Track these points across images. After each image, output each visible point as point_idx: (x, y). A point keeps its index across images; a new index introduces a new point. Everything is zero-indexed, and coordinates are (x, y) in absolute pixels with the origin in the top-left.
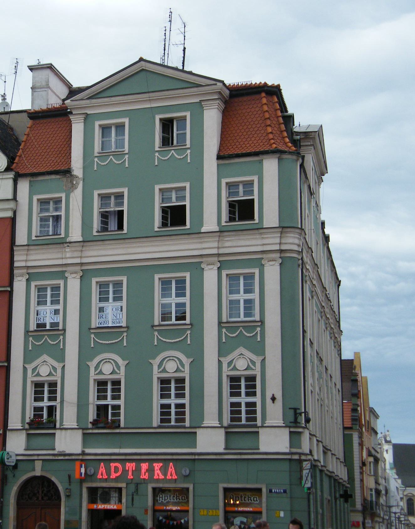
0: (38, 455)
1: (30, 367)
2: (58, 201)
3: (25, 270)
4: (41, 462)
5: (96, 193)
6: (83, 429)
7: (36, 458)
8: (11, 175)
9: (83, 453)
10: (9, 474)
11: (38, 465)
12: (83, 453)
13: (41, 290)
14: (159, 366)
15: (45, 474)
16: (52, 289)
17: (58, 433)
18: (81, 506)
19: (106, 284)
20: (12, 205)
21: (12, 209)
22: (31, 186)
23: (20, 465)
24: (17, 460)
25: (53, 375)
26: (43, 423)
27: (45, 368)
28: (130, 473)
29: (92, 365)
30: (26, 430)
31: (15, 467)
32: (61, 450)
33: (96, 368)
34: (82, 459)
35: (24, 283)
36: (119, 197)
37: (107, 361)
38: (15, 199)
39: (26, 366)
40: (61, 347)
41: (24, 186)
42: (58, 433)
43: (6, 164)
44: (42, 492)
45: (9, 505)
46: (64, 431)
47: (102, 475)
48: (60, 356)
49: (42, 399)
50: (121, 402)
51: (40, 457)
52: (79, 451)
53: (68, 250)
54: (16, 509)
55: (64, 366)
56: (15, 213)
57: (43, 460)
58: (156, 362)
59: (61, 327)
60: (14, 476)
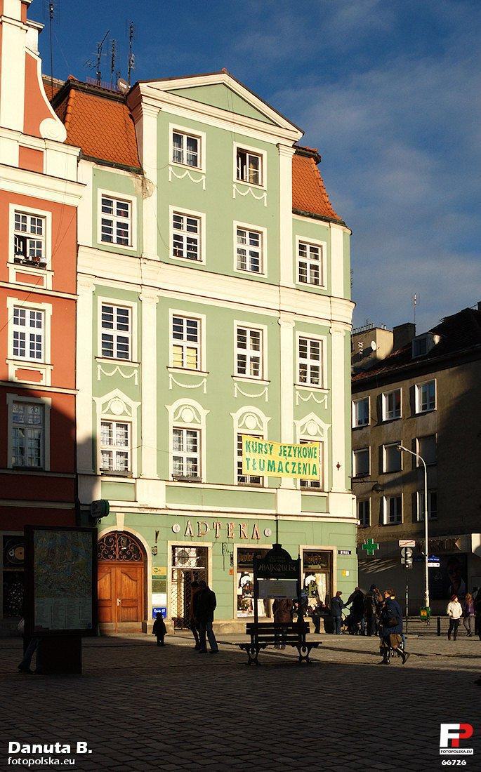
14: (240, 421)
25: (127, 415)
29: (171, 409)
33: (176, 413)
40: (136, 383)
43: (40, 128)
44: (120, 549)
48: (136, 393)
58: (236, 416)
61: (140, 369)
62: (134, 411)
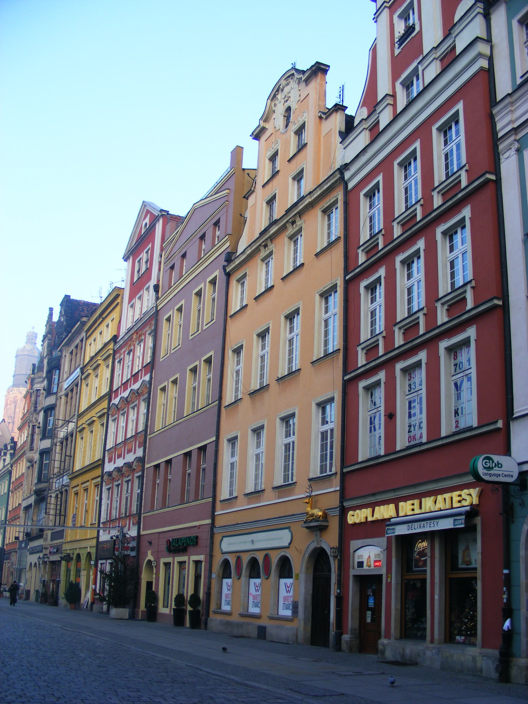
3: (512, 138)
56: (491, 59)
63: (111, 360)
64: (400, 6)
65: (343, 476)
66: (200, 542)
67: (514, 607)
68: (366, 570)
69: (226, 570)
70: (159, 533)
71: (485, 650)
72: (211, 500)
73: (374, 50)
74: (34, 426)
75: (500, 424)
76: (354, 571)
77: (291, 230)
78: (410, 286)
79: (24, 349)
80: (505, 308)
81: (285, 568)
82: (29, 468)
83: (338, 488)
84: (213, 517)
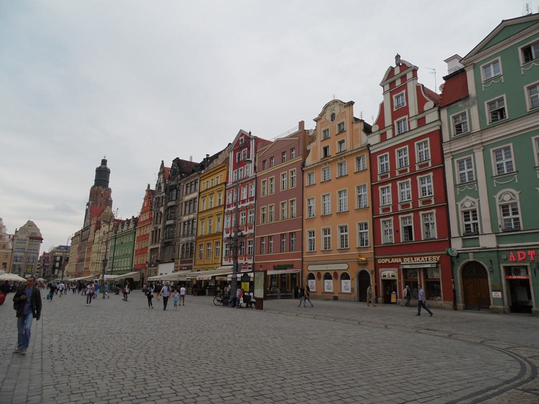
0: (470, 250)
1: (459, 204)
2: (464, 114)
4: (472, 253)
5: (486, 103)
6: (496, 233)
7: (469, 251)
8: (436, 109)
9: (498, 247)
10: (455, 260)
11: (471, 255)
12: (498, 247)
13: (461, 162)
15: (475, 260)
16: (467, 161)
17: (480, 237)
18: (501, 277)
19: (500, 150)
20: (438, 123)
21: (438, 125)
22: (448, 112)
23: (460, 255)
24: (458, 253)
25: (473, 206)
26: (471, 233)
27: (468, 203)
28: (532, 257)
29: (497, 197)
30: (462, 237)
31: (458, 257)
32: (484, 246)
33: (500, 198)
34: (498, 251)
35: (450, 161)
36: (501, 100)
37: (507, 193)
38: (440, 119)
39: (457, 203)
41: (444, 113)
42: (480, 237)
45: (457, 278)
46: (484, 236)
47: (512, 259)
48: (476, 195)
49: (469, 220)
50: (519, 216)
51: (471, 251)
52: (495, 246)
53: (473, 137)
54: (462, 280)
55: (479, 200)
56: (441, 127)
57: (473, 252)
59: (474, 180)
60: (458, 262)
61: (477, 183)
62: (477, 203)
63: (222, 193)
64: (397, 93)
65: (374, 248)
66: (294, 266)
67: (456, 289)
68: (387, 278)
69: (311, 276)
70: (267, 263)
71: (445, 302)
72: (301, 251)
73: (382, 106)
74: (157, 213)
75: (447, 239)
76: (381, 278)
77: (339, 161)
78: (405, 192)
79: (100, 167)
80: (447, 206)
81: (345, 276)
82: (153, 231)
83: (373, 251)
84: (302, 258)
